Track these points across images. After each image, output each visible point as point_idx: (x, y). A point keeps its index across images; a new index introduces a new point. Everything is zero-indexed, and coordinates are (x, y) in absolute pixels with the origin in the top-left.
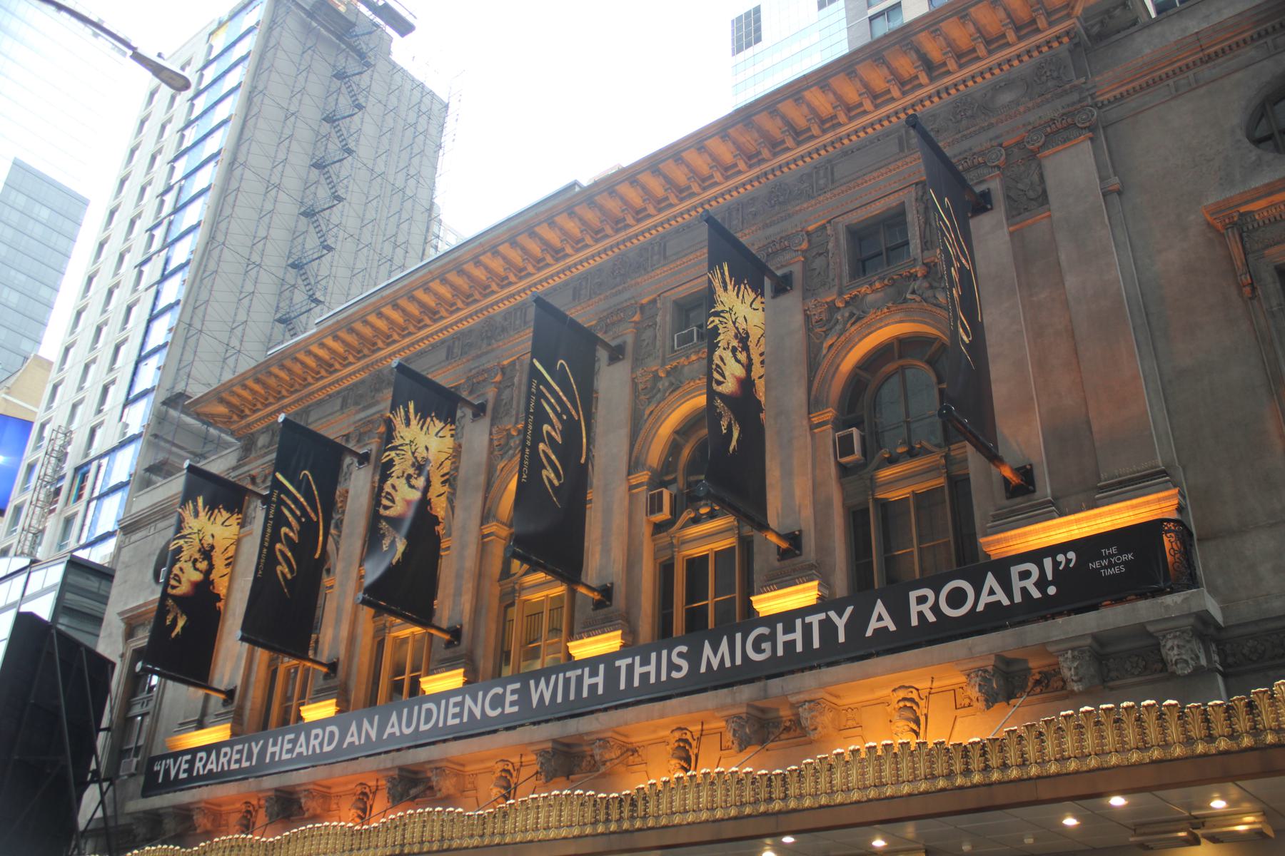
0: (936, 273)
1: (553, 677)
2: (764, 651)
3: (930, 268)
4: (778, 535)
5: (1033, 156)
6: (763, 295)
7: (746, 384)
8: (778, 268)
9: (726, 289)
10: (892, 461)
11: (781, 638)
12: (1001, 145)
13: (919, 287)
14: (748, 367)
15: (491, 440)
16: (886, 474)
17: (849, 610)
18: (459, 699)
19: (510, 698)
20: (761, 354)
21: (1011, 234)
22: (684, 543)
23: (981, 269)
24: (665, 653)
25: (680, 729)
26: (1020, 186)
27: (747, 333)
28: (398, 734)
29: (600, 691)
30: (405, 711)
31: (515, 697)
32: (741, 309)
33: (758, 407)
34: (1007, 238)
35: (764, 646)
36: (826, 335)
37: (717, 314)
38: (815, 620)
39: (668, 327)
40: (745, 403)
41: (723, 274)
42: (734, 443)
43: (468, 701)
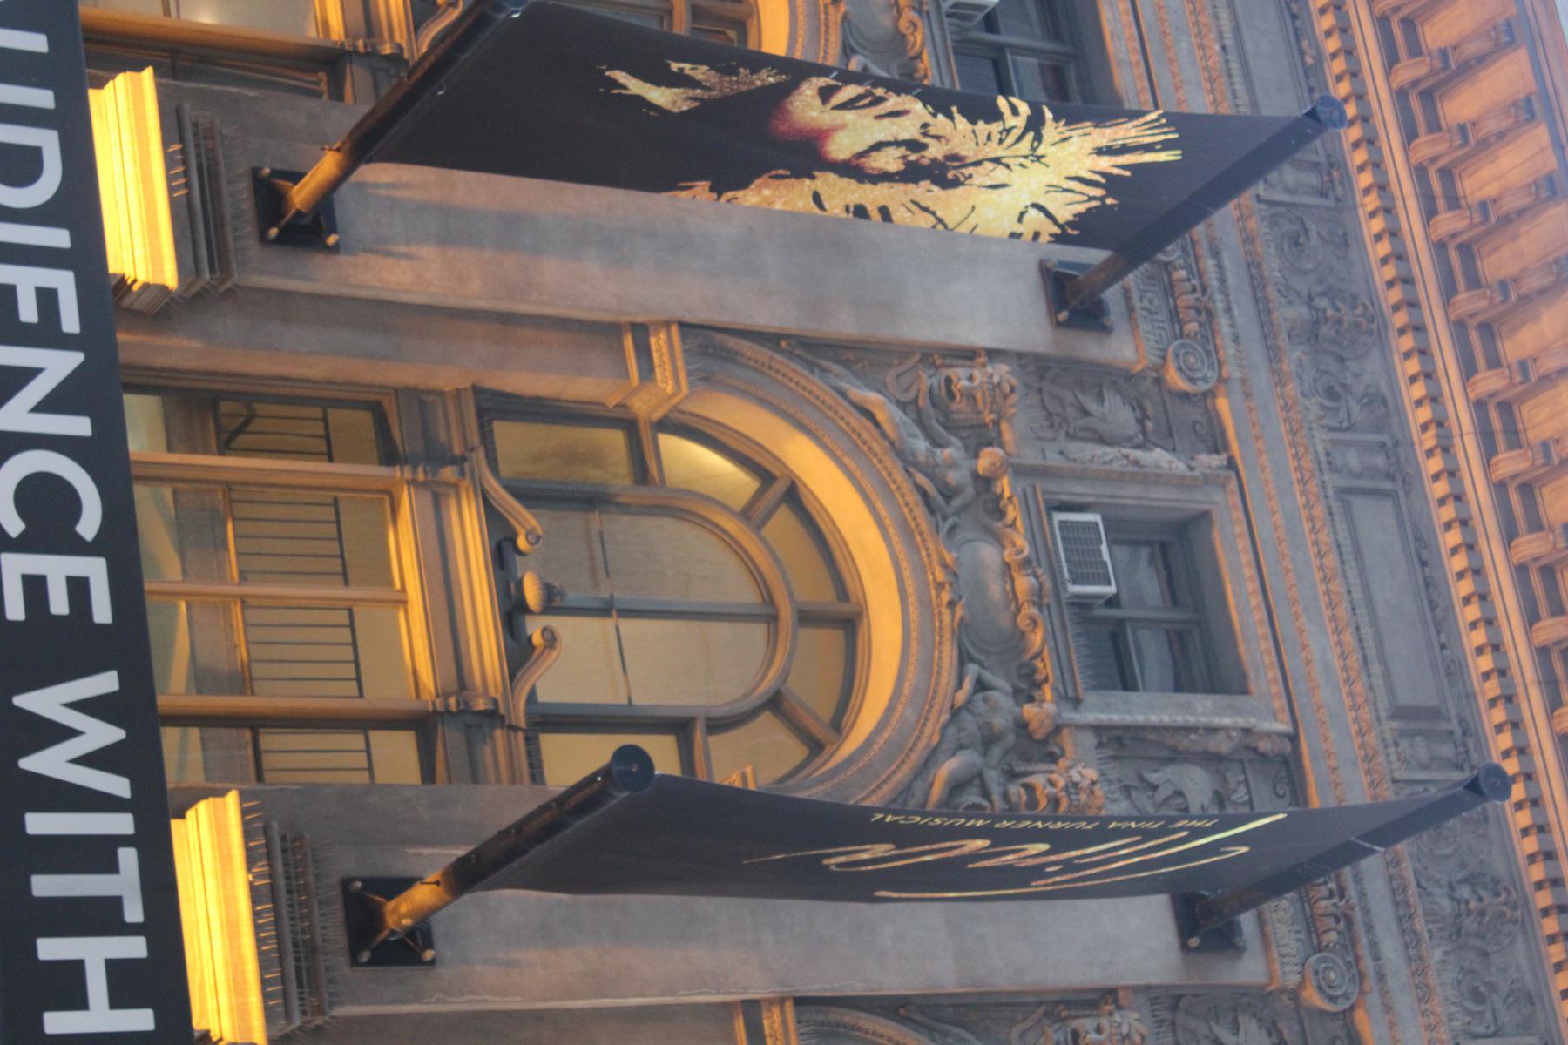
1: (118, 786)
6: (1059, 239)
7: (805, 156)
8: (1126, 292)
9: (1100, 152)
10: (502, 552)
13: (994, 708)
14: (852, 169)
15: (968, 355)
16: (469, 532)
18: (70, 322)
19: (57, 569)
20: (885, 213)
22: (437, 502)
27: (955, 183)
29: (57, 1022)
30: (36, 43)
31: (59, 604)
32: (1036, 177)
33: (729, 179)
36: (903, 406)
37: (1035, 124)
39: (1129, 494)
40: (745, 137)
41: (1149, 148)
42: (635, 86)
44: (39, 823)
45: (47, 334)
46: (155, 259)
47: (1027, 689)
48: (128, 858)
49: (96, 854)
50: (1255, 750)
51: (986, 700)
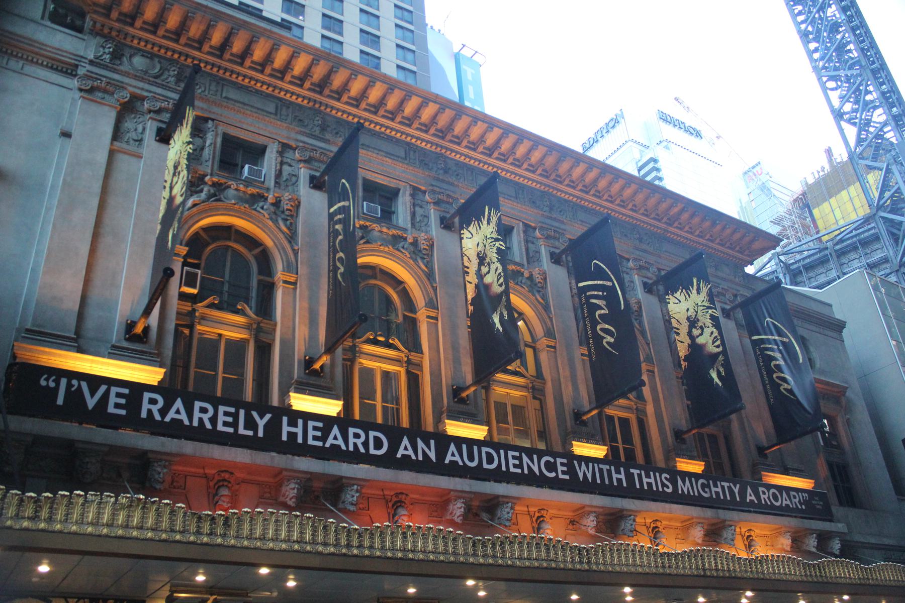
2: (706, 492)
11: (714, 489)
17: (738, 486)
18: (517, 454)
19: (560, 468)
24: (657, 474)
25: (656, 520)
28: (461, 463)
31: (565, 469)
35: (707, 490)
38: (726, 484)
43: (525, 459)
44: (599, 481)
45: (520, 458)
46: (483, 430)
48: (601, 466)
49: (601, 470)
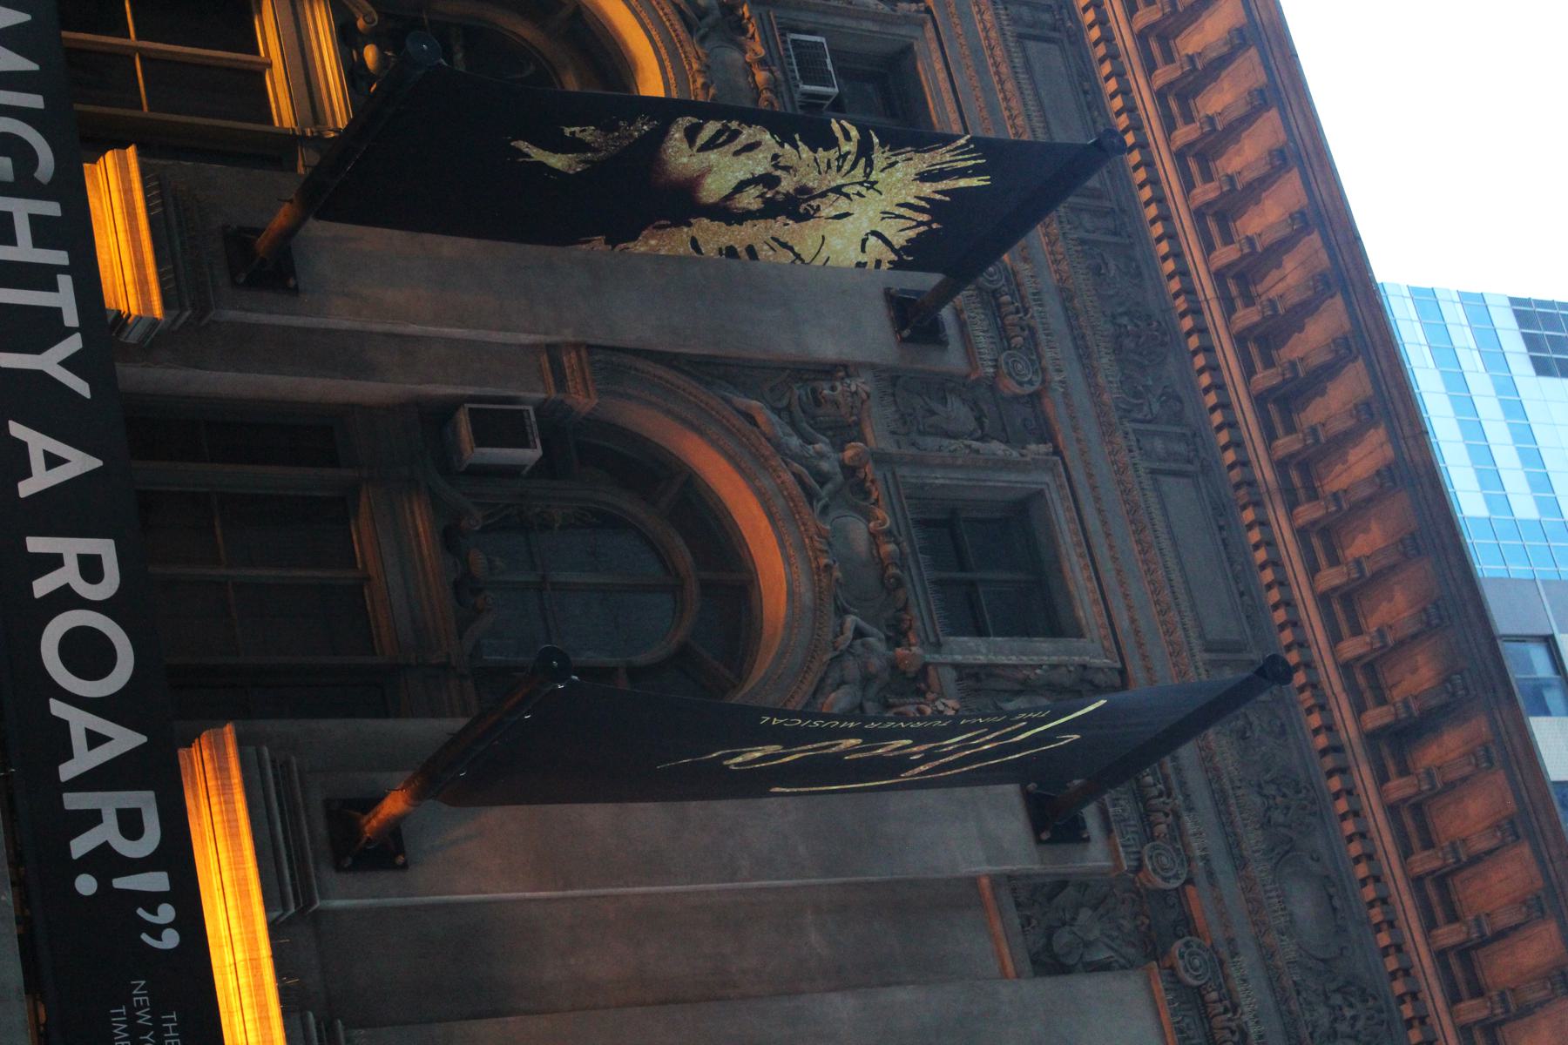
0: (902, 695)
3: (915, 682)
4: (289, 233)
5: (1151, 948)
12: (1189, 881)
21: (973, 881)
23: (900, 803)
26: (1085, 915)
34: (964, 870)
47: (897, 636)
50: (1091, 682)
51: (863, 645)
